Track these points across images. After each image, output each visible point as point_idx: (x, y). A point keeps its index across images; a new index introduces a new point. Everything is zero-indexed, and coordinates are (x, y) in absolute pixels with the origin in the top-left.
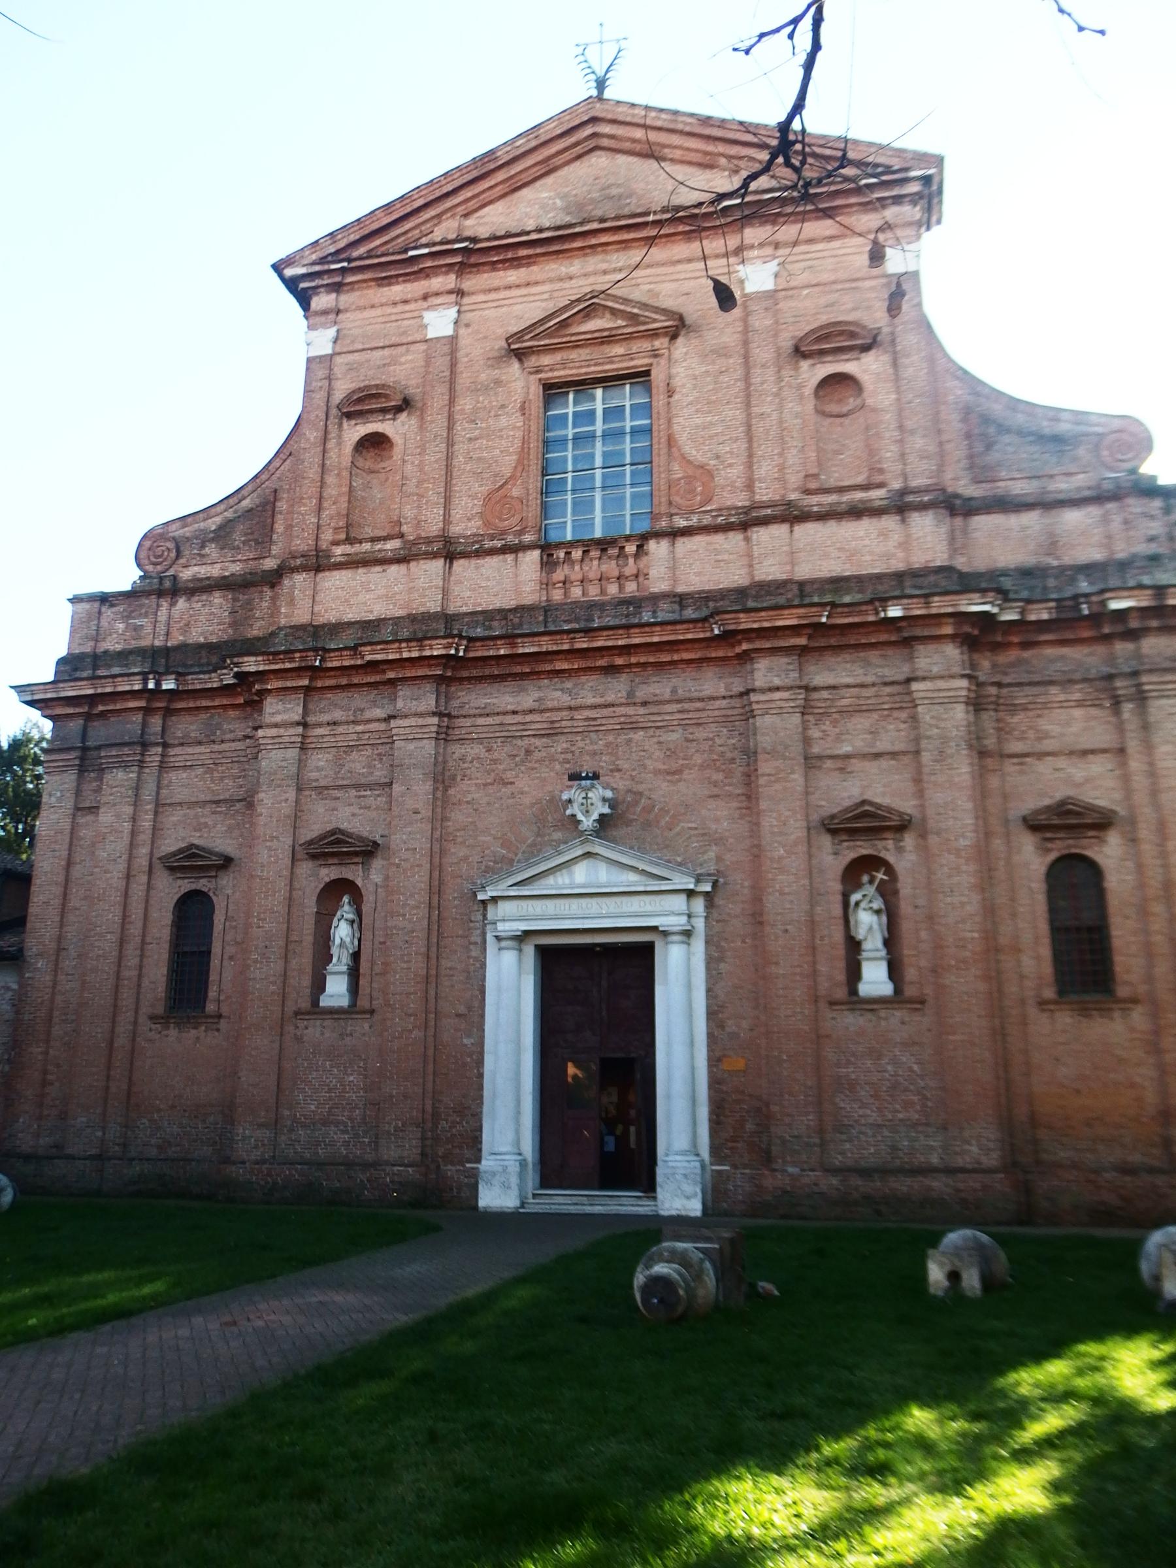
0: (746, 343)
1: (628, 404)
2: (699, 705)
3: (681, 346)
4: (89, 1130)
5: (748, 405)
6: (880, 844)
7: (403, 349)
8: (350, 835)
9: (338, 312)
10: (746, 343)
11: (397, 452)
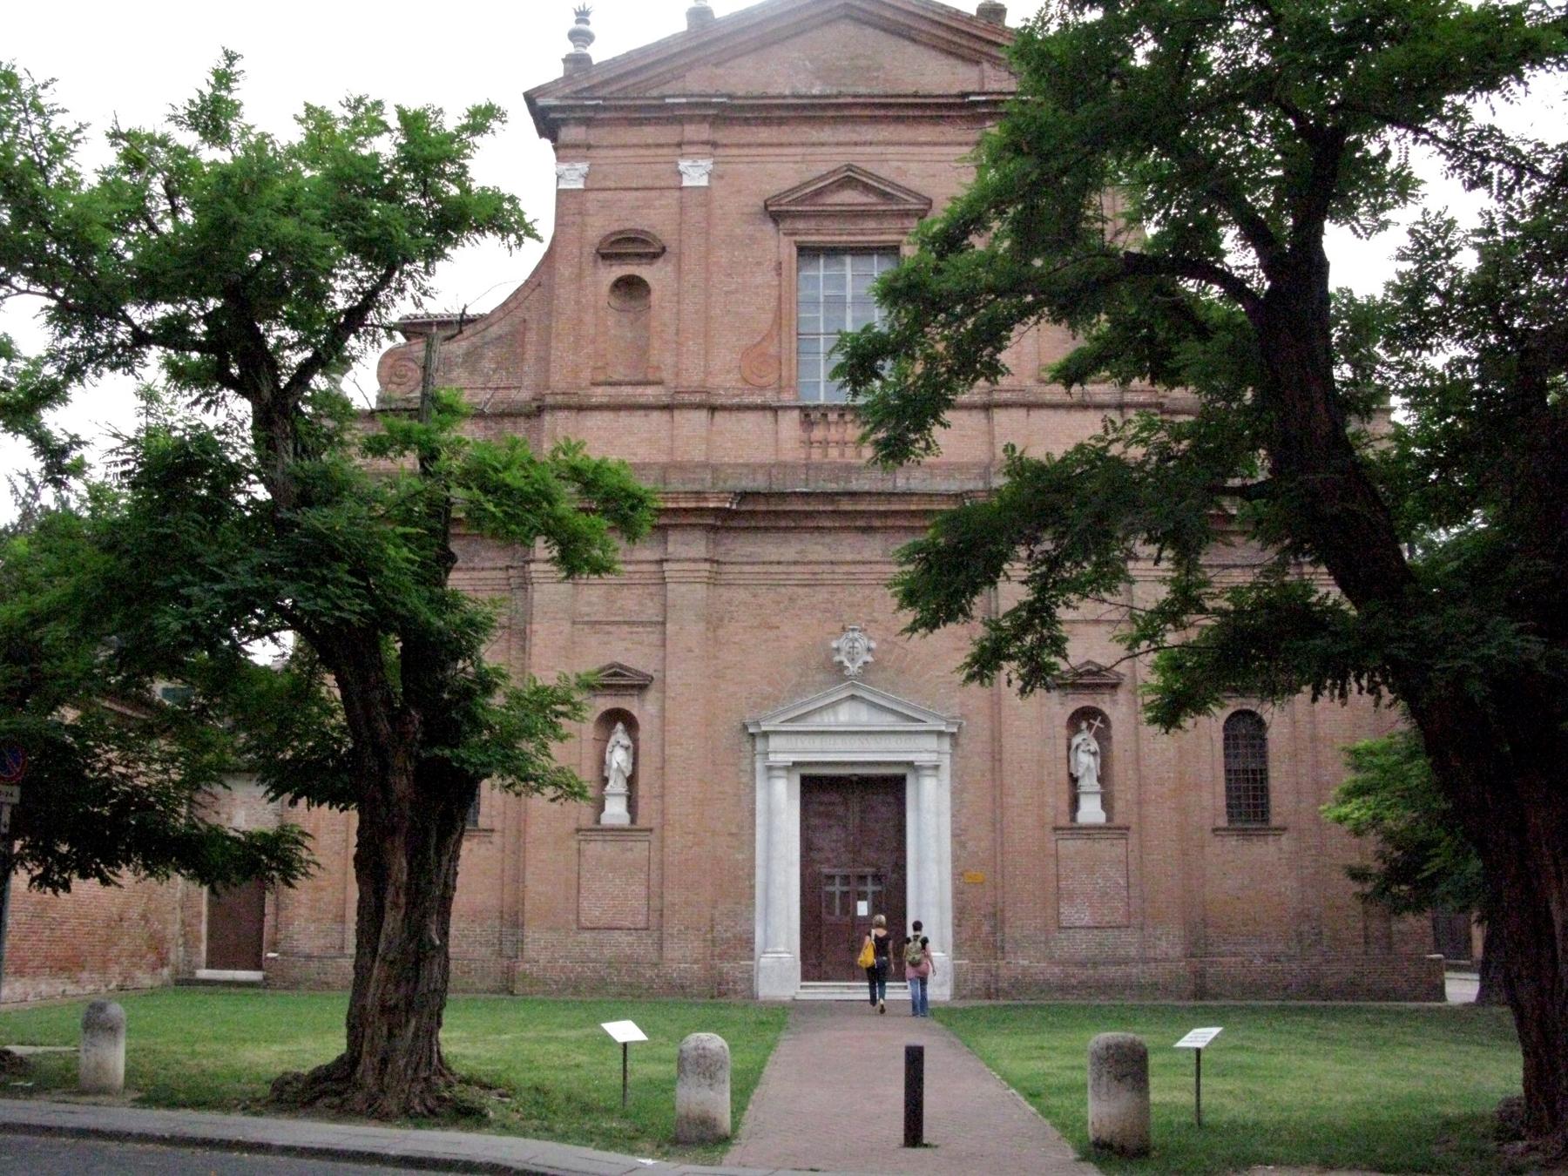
6: (1099, 698)
7: (653, 194)
8: (628, 669)
9: (589, 147)
11: (654, 298)
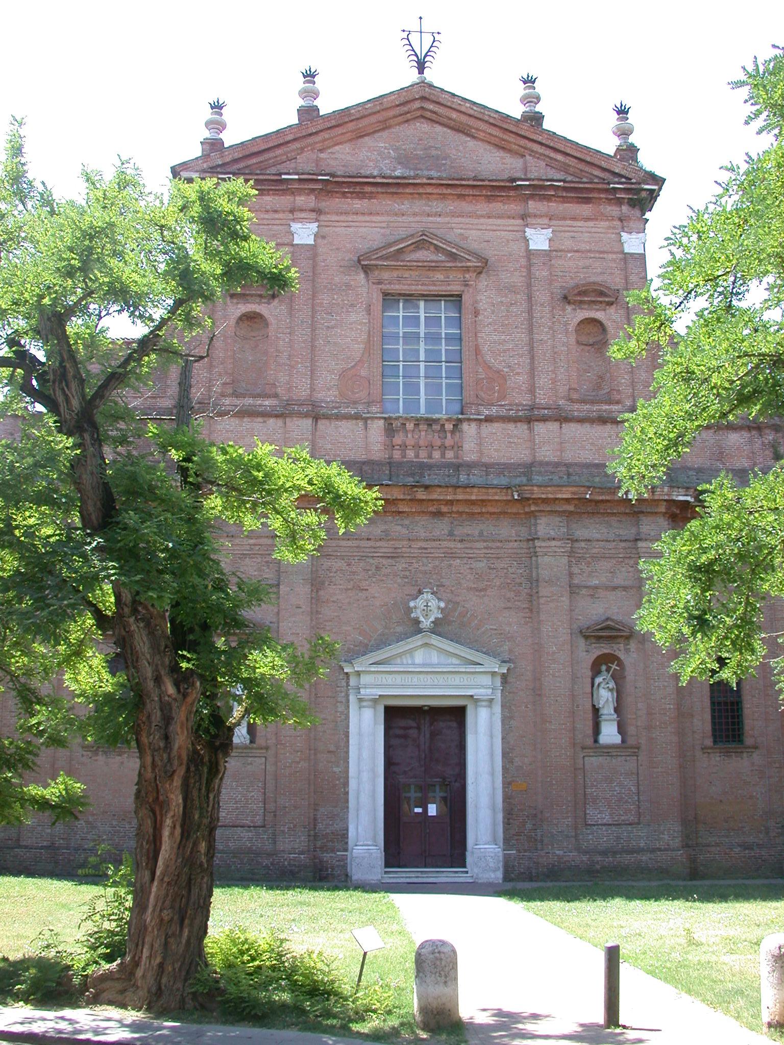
0: (529, 286)
1: (443, 316)
2: (499, 544)
3: (483, 282)
4: (40, 828)
5: (531, 331)
6: (615, 646)
10: (529, 286)
